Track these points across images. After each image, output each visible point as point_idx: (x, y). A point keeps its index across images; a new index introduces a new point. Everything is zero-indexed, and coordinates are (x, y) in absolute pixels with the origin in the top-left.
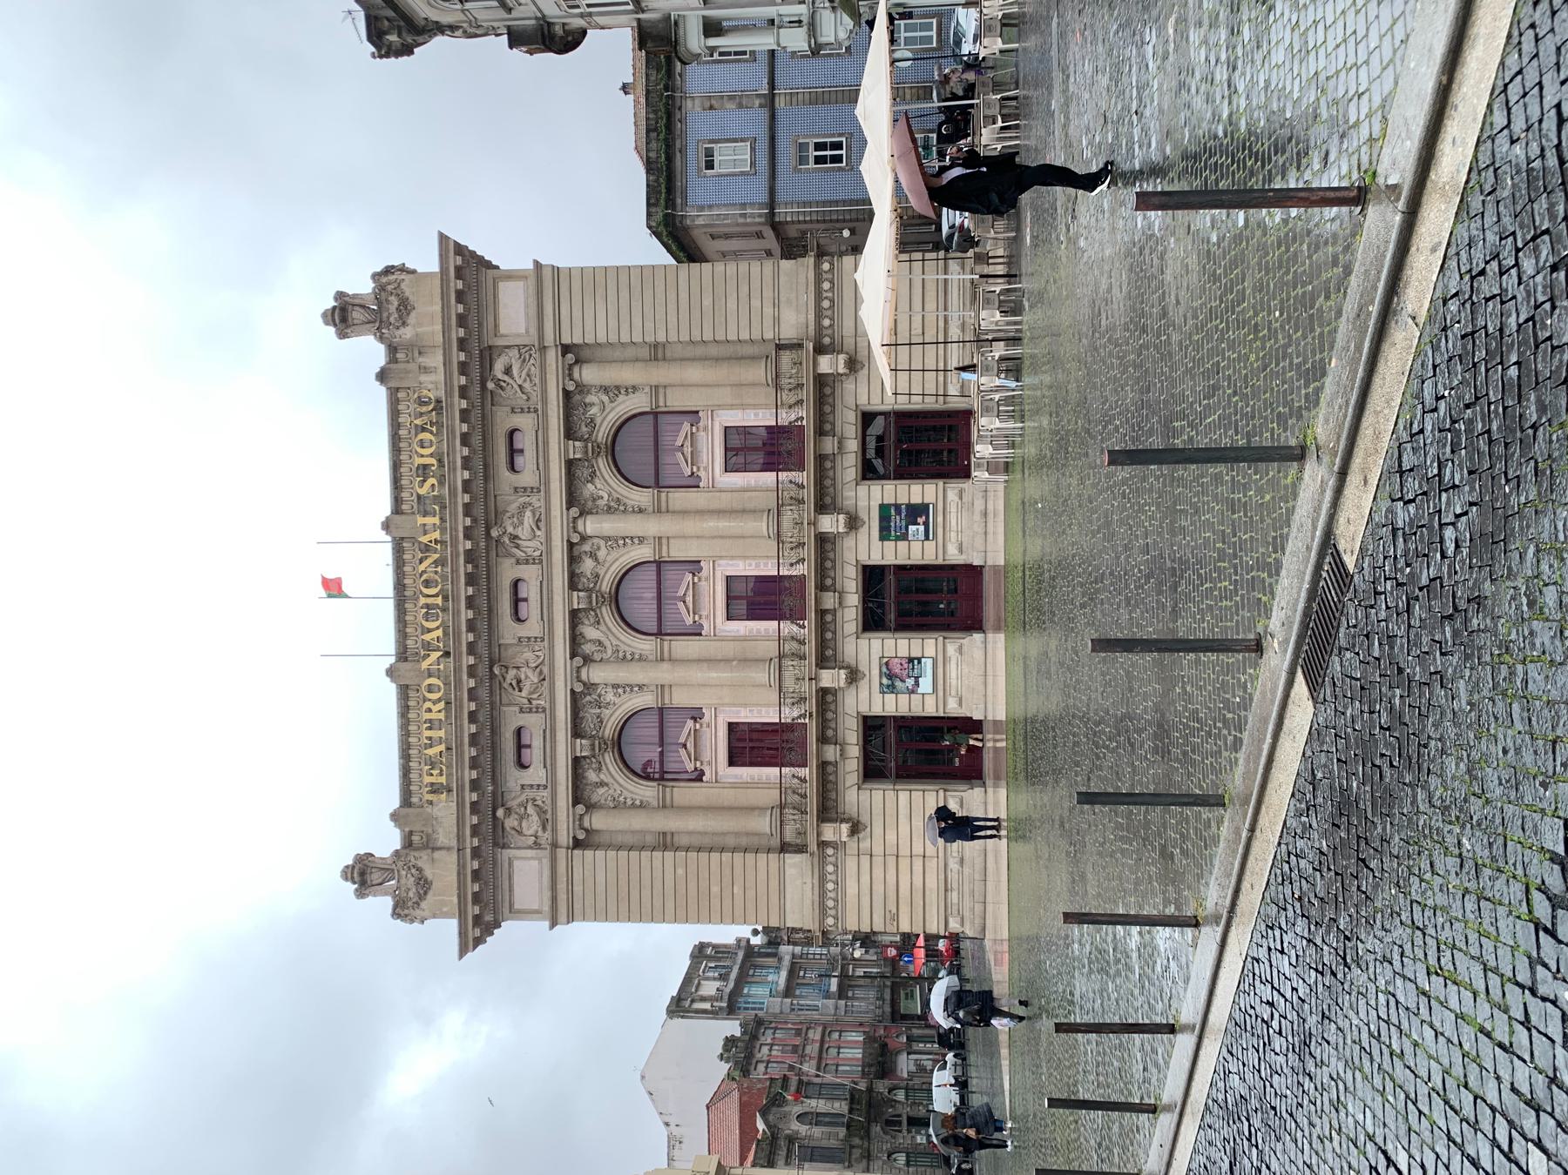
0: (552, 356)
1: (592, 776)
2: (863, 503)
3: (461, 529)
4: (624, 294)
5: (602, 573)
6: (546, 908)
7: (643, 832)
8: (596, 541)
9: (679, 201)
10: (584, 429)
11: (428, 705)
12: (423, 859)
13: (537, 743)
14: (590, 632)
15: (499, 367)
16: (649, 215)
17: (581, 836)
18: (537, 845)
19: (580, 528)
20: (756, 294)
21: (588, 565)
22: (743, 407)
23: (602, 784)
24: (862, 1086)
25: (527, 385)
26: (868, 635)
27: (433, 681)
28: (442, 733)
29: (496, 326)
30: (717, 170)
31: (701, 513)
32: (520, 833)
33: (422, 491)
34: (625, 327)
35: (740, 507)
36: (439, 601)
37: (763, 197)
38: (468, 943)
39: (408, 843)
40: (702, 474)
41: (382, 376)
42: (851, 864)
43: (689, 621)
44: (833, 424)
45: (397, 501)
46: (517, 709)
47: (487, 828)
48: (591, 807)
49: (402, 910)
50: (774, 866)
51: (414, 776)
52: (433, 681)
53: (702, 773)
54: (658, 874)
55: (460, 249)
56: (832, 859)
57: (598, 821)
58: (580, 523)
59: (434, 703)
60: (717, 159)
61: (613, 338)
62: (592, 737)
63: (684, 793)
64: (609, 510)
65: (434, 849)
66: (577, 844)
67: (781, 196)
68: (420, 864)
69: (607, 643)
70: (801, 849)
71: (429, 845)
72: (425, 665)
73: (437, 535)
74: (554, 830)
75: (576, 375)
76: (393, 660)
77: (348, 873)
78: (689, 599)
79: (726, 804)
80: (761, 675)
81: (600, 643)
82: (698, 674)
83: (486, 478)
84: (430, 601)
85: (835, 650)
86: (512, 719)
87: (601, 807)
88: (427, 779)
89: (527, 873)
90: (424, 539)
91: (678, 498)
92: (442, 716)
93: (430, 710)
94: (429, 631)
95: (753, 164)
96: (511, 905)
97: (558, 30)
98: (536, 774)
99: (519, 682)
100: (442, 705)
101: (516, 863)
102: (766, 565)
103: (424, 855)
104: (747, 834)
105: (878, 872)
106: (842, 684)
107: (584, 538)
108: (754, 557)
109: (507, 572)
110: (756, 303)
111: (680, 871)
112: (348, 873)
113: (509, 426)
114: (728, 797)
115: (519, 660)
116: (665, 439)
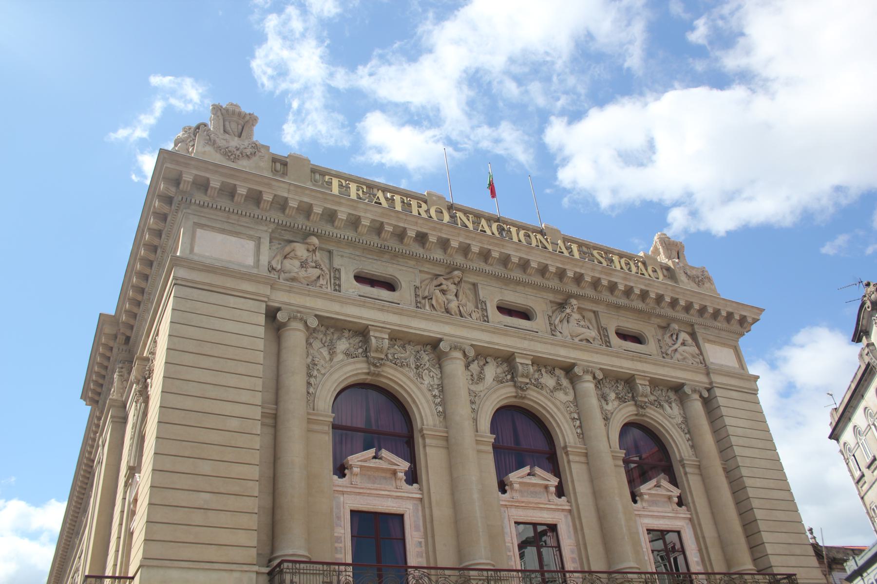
1: (342, 345)
5: (544, 392)
8: (572, 392)
13: (384, 294)
25: (677, 356)
32: (285, 257)
47: (301, 221)
53: (343, 475)
54: (232, 395)
78: (533, 480)
96: (202, 226)
111: (234, 424)
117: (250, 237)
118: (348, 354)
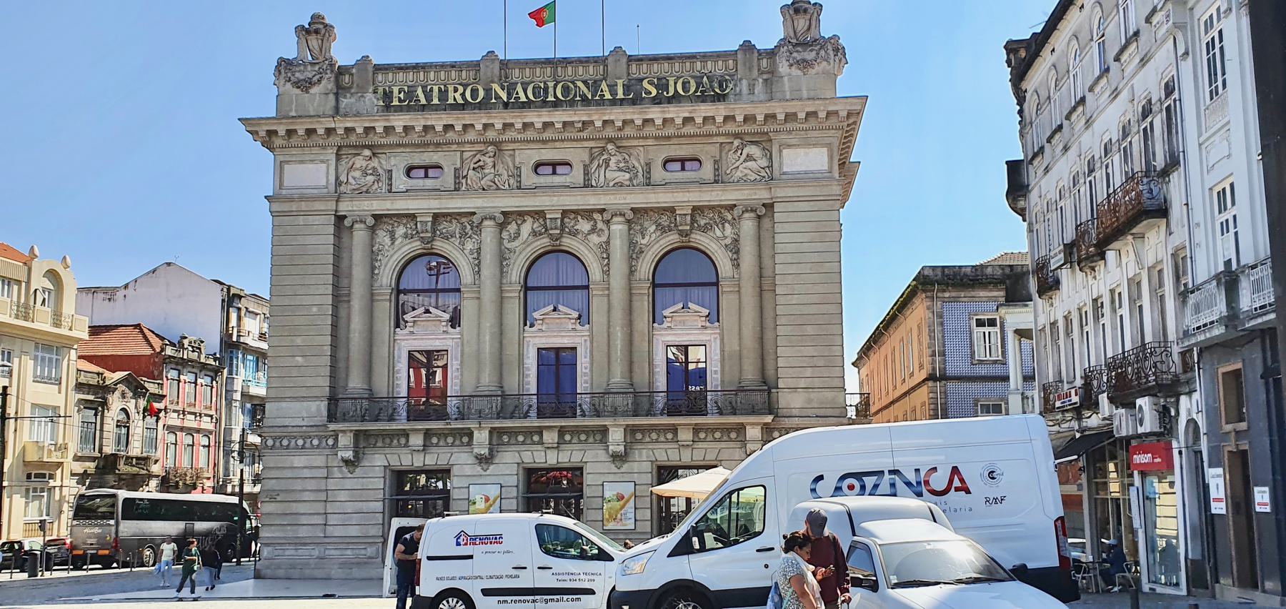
0: (763, 195)
1: (401, 231)
2: (636, 467)
3: (612, 118)
4: (815, 258)
6: (284, 192)
7: (350, 275)
8: (606, 232)
9: (947, 295)
10: (702, 222)
11: (461, 89)
12: (327, 84)
13: (429, 183)
14: (526, 228)
15: (754, 150)
16: (934, 268)
17: (347, 223)
18: (338, 183)
19: (615, 219)
20: (817, 372)
21: (584, 226)
22: (723, 360)
23: (393, 239)
24: (156, 469)
26: (521, 472)
27: (481, 93)
28: (436, 101)
29: (789, 146)
30: (978, 331)
31: (630, 324)
33: (645, 83)
34: (789, 258)
35: (635, 359)
36: (551, 98)
37: (949, 372)
38: (250, 124)
39: (342, 71)
40: (665, 325)
41: (747, 47)
42: (319, 460)
43: (536, 315)
44: (704, 441)
45: (640, 60)
46: (458, 165)
48: (373, 229)
49: (284, 66)
50: (317, 392)
51: (401, 76)
52: (481, 93)
55: (859, 113)
56: (324, 444)
57: (360, 235)
58: (621, 219)
59: (463, 95)
60: (987, 329)
61: (779, 248)
62: (434, 232)
63: (385, 310)
64: (632, 244)
65: (337, 95)
66: (340, 219)
67: (951, 385)
68: (323, 82)
69: (516, 243)
70: (332, 417)
71: (340, 90)
72: (496, 87)
73: (608, 96)
74: (352, 200)
75: (746, 215)
76: (501, 57)
77: (316, 18)
79: (375, 349)
80: (488, 380)
81: (518, 234)
82: (489, 323)
83: (656, 138)
84: (551, 90)
85: (508, 444)
86: (449, 160)
87: (372, 239)
88: (396, 90)
89: (313, 173)
90: (604, 86)
91: (643, 306)
92: (451, 101)
93: (456, 90)
94: (525, 91)
95: (981, 362)
96: (287, 162)
97: (1021, 204)
98: (401, 182)
99: (482, 167)
100: (460, 101)
101: (324, 166)
102: (586, 382)
103: (331, 86)
104: (347, 368)
105: (312, 485)
106: (476, 450)
107: (608, 222)
108: (592, 371)
109: (576, 155)
110: (809, 372)
112: (316, 18)
113: (702, 158)
114: (382, 351)
115: (500, 167)
116: (695, 291)
117: (322, 162)
118: (406, 236)
